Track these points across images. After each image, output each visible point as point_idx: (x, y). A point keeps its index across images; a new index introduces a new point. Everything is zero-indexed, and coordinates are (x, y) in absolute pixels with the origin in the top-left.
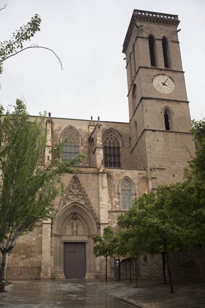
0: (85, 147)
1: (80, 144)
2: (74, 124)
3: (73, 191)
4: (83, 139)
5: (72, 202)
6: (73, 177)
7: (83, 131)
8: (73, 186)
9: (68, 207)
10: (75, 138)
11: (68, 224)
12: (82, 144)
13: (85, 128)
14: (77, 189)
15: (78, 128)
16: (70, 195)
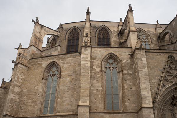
0: (155, 45)
1: (150, 42)
2: (141, 27)
3: (170, 71)
4: (153, 39)
5: (173, 83)
6: (169, 57)
7: (151, 32)
8: (170, 67)
9: (169, 90)
10: (144, 38)
11: (167, 110)
12: (152, 42)
13: (152, 30)
14: (175, 69)
15: (146, 30)
16: (168, 76)
